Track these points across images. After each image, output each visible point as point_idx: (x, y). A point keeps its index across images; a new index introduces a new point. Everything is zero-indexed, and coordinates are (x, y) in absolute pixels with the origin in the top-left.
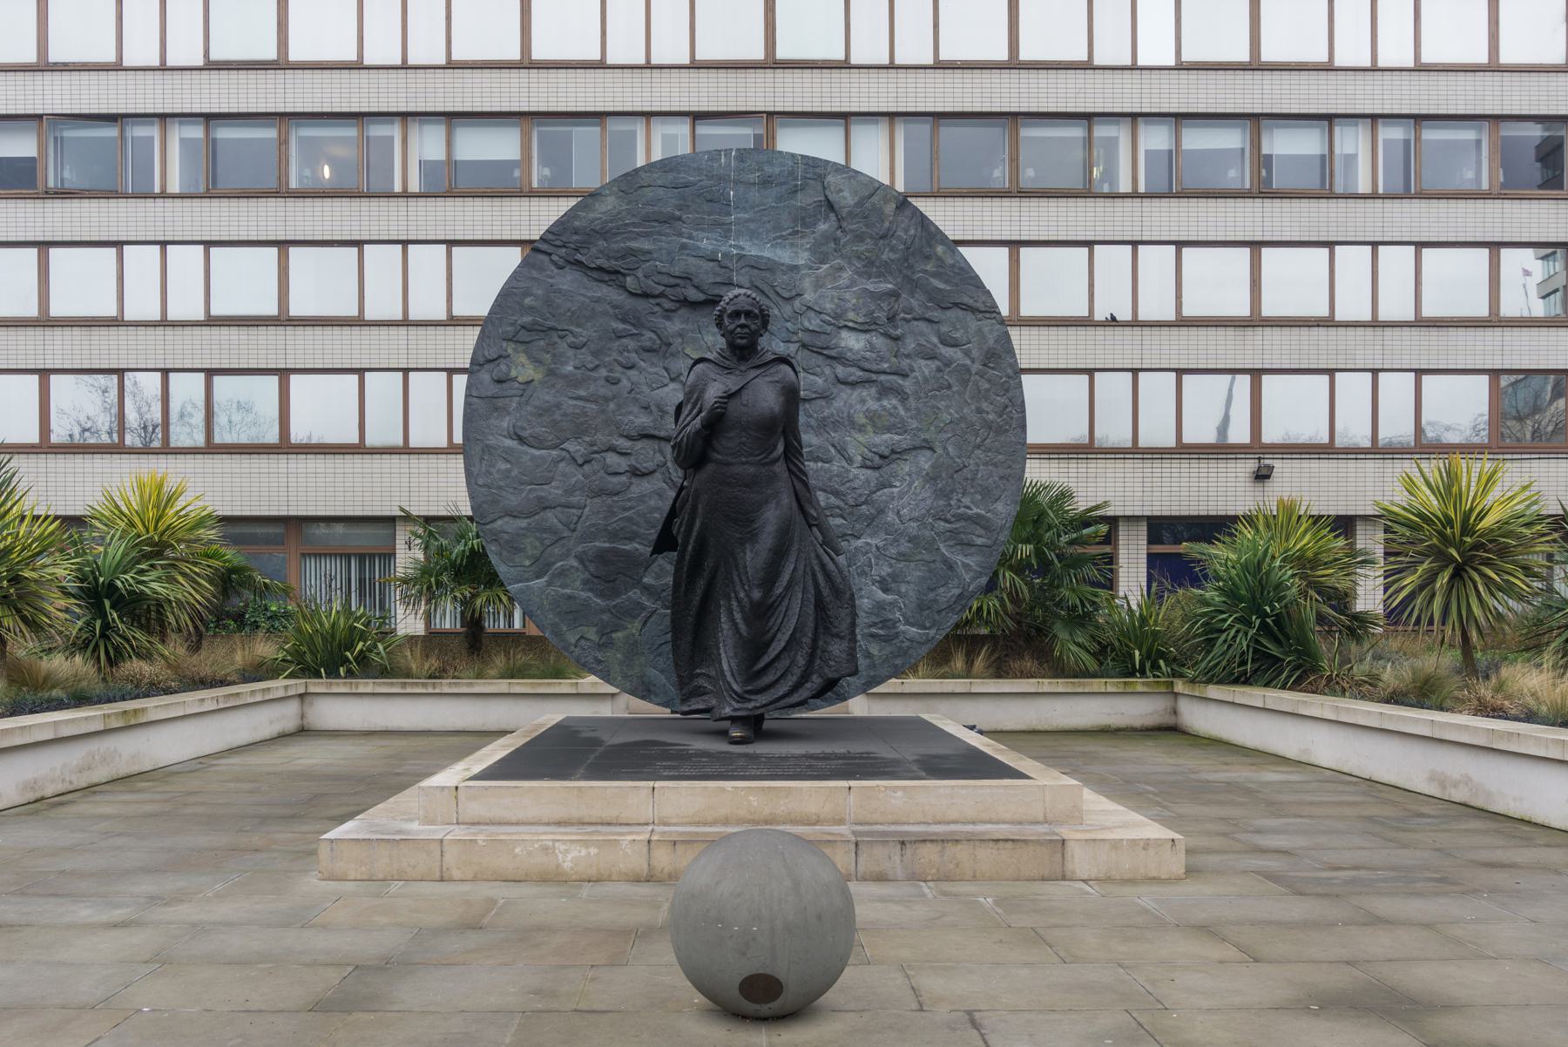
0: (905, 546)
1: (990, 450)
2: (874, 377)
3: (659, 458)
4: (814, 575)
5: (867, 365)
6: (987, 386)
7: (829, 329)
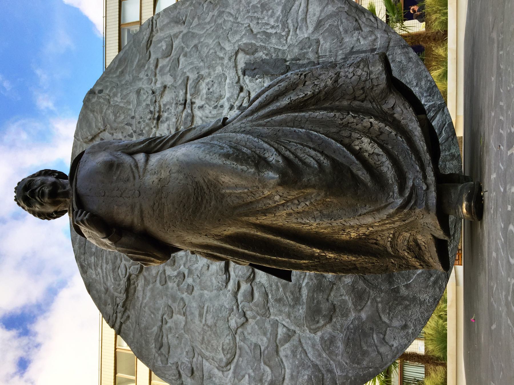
1: (238, 10)
6: (196, 20)
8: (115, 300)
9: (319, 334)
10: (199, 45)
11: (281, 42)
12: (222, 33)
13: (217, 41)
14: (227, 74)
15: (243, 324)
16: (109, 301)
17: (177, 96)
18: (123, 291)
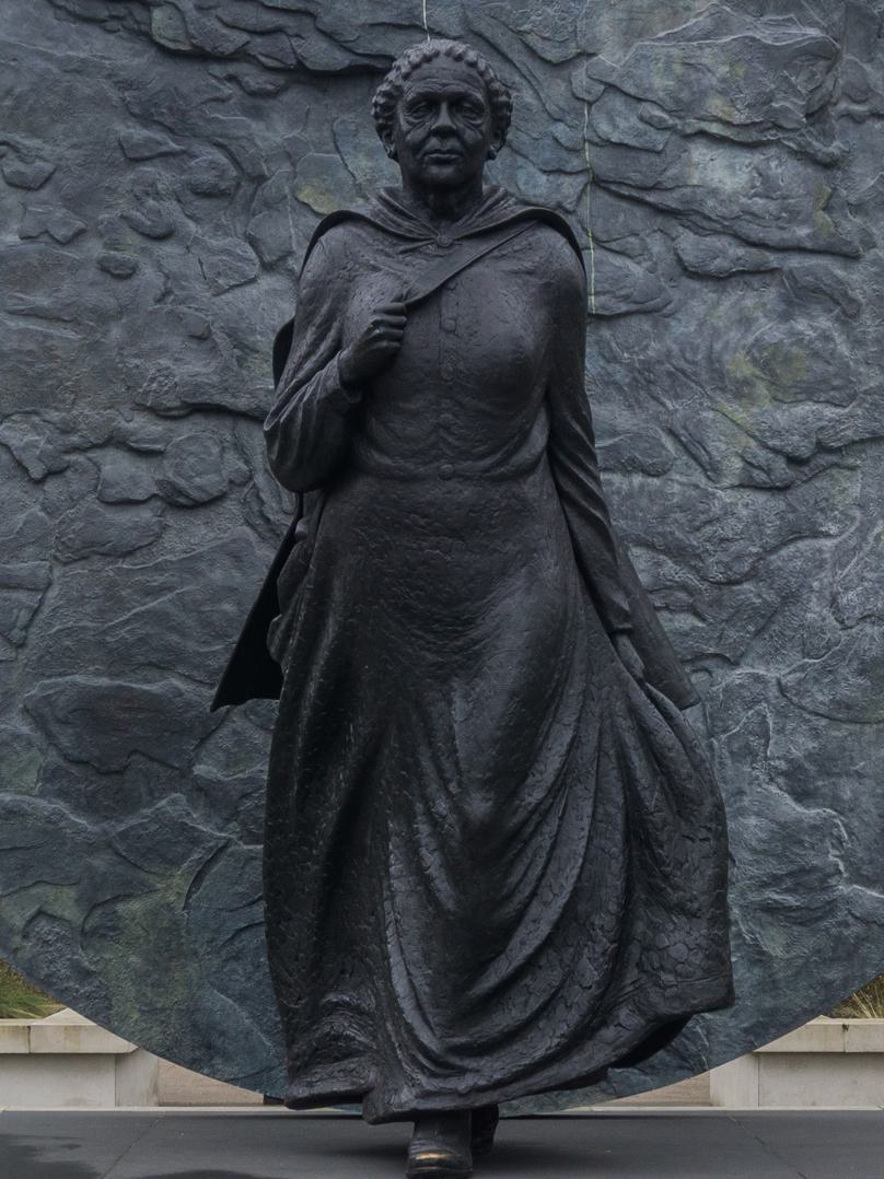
0: (851, 685)
2: (773, 260)
3: (234, 463)
4: (623, 758)
5: (754, 231)
7: (659, 139)
15: (21, 466)
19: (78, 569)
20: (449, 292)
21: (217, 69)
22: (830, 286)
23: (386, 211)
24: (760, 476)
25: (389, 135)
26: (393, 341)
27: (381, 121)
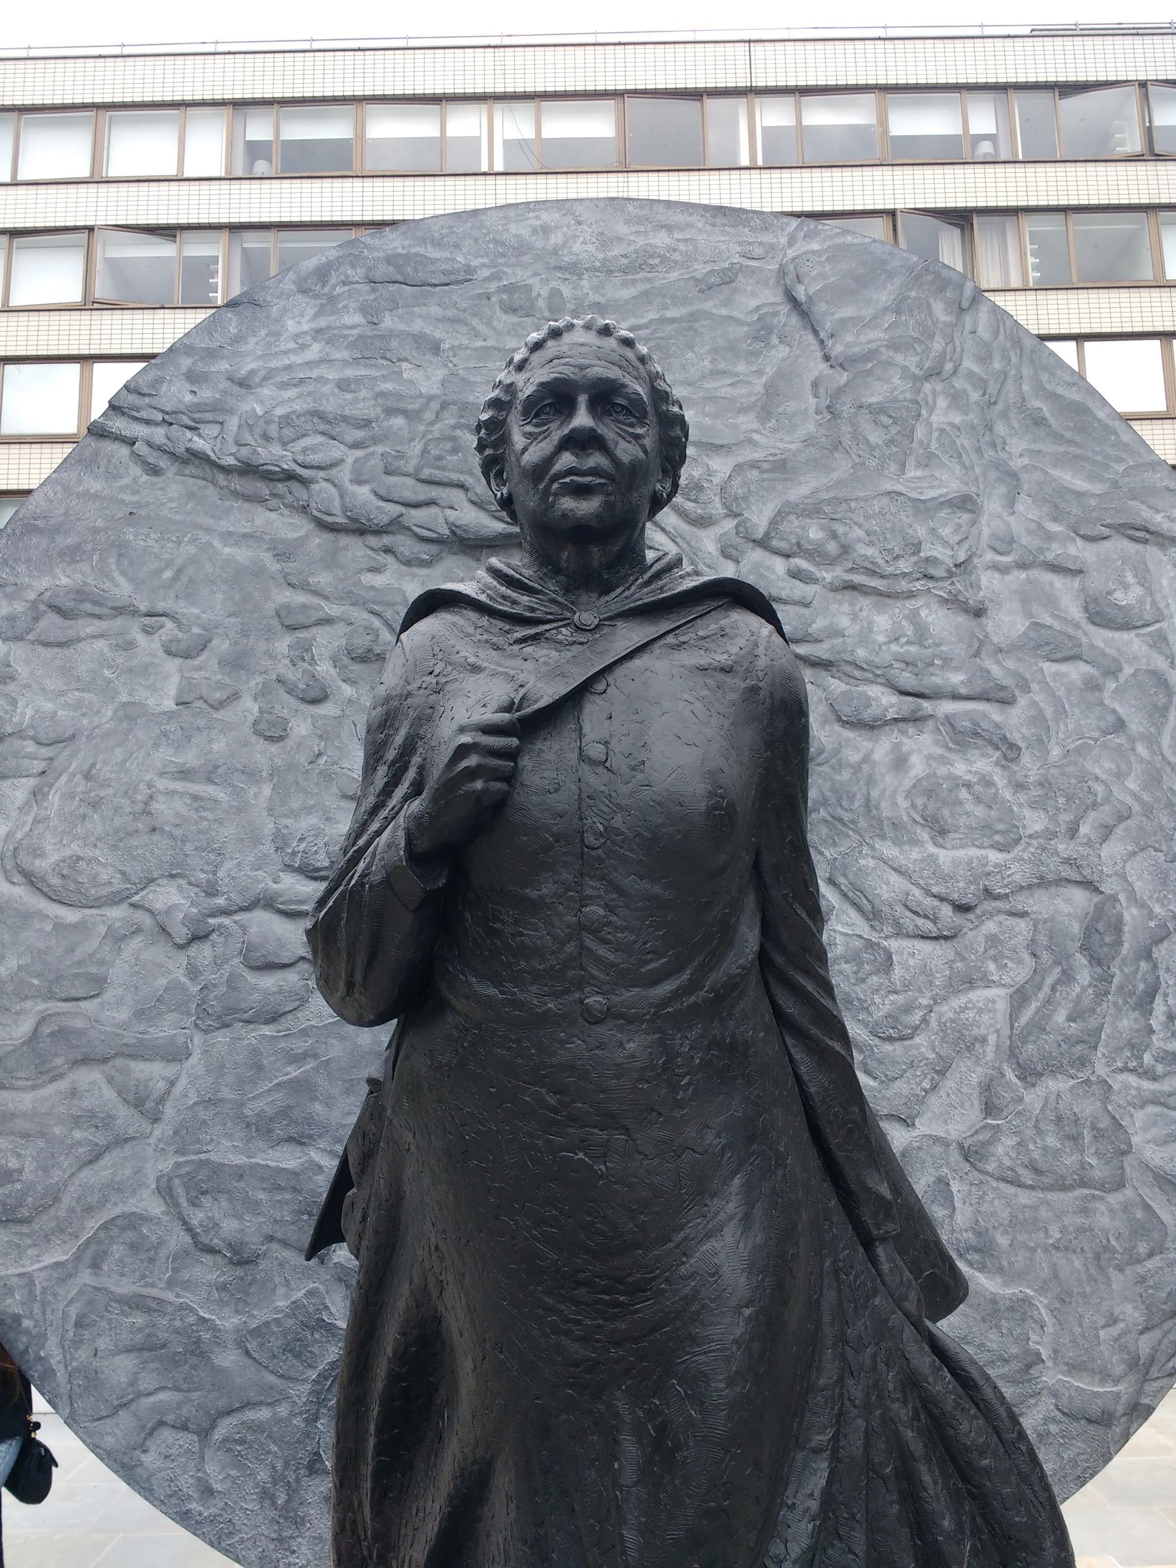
8: (208, 416)
9: (156, 1207)
10: (1120, 740)
11: (1119, 1049)
12: (1161, 827)
13: (1136, 807)
14: (1017, 850)
16: (206, 394)
17: (947, 662)
18: (244, 452)
19: (221, 1038)
20: (597, 699)
21: (373, 541)
22: (988, 731)
23: (495, 583)
24: (927, 926)
25: (499, 475)
26: (497, 779)
27: (488, 452)
